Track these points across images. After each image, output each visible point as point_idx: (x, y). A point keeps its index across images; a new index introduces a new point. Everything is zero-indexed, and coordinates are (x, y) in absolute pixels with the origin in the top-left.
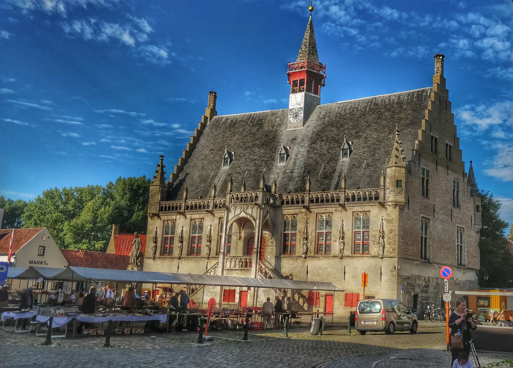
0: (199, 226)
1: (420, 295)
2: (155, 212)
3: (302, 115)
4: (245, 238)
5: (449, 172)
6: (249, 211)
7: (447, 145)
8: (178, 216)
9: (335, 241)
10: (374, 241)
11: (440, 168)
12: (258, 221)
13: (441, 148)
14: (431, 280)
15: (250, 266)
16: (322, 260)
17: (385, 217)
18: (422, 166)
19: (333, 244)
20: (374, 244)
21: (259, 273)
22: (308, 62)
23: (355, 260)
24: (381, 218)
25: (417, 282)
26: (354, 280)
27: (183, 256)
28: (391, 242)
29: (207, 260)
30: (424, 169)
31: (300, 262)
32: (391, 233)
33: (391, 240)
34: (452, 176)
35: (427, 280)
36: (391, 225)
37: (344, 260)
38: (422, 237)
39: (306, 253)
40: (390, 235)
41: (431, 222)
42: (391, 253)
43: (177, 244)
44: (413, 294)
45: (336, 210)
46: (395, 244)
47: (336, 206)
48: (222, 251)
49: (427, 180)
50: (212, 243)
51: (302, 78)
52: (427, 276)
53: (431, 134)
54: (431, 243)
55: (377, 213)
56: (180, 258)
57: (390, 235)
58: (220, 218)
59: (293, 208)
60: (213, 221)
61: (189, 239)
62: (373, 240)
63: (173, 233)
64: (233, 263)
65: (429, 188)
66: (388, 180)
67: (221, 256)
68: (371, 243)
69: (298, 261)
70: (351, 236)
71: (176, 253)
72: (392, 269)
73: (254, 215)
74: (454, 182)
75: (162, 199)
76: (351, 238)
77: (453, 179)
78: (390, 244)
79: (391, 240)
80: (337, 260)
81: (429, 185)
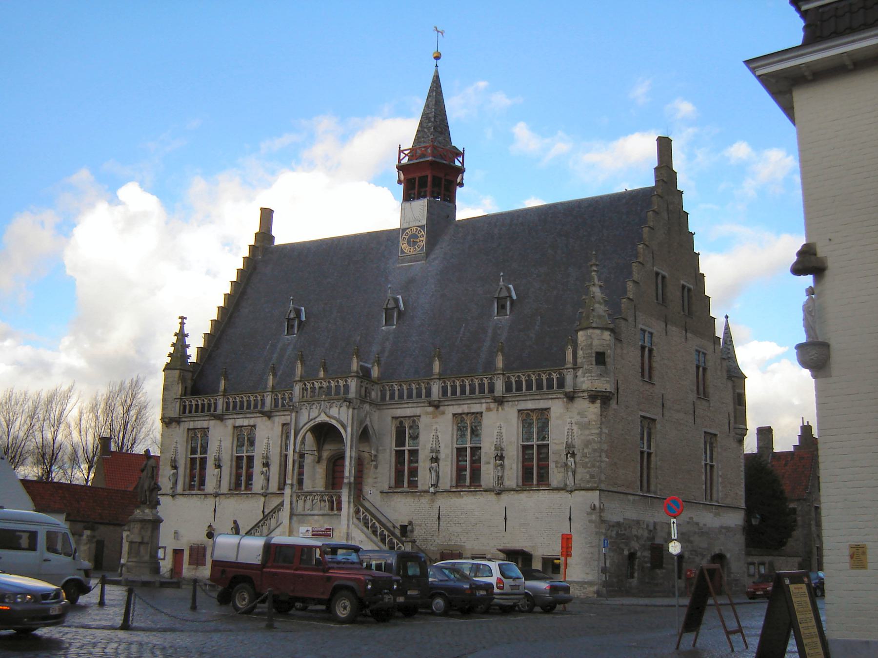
0: (248, 439)
1: (639, 554)
2: (173, 415)
3: (424, 239)
4: (329, 460)
5: (689, 335)
6: (334, 411)
7: (684, 287)
8: (212, 423)
9: (488, 463)
10: (557, 462)
11: (673, 329)
12: (349, 429)
13: (674, 294)
14: (658, 528)
15: (339, 509)
16: (465, 497)
17: (577, 418)
18: (641, 326)
19: (484, 468)
21: (355, 520)
22: (434, 148)
23: (523, 496)
25: (634, 532)
26: (524, 530)
28: (587, 463)
29: (263, 499)
30: (644, 331)
31: (425, 500)
33: (587, 460)
34: (695, 342)
35: (651, 528)
36: (587, 432)
37: (505, 497)
38: (642, 453)
39: (435, 485)
40: (586, 451)
41: (658, 426)
42: (588, 482)
43: (211, 471)
44: (626, 553)
47: (488, 401)
48: (289, 481)
49: (651, 351)
50: (271, 467)
51: (423, 174)
52: (651, 520)
53: (655, 269)
54: (659, 463)
56: (216, 495)
57: (586, 451)
58: (284, 425)
59: (410, 405)
60: (272, 429)
61: (232, 460)
62: (555, 459)
63: (204, 450)
64: (309, 502)
65: (654, 365)
66: (580, 353)
67: (288, 491)
68: (552, 465)
70: (515, 453)
71: (210, 485)
72: (589, 510)
73: (344, 419)
74: (698, 352)
75: (185, 394)
76: (515, 457)
77: (695, 348)
78: (585, 466)
79: (587, 460)
80: (492, 497)
81: (655, 359)
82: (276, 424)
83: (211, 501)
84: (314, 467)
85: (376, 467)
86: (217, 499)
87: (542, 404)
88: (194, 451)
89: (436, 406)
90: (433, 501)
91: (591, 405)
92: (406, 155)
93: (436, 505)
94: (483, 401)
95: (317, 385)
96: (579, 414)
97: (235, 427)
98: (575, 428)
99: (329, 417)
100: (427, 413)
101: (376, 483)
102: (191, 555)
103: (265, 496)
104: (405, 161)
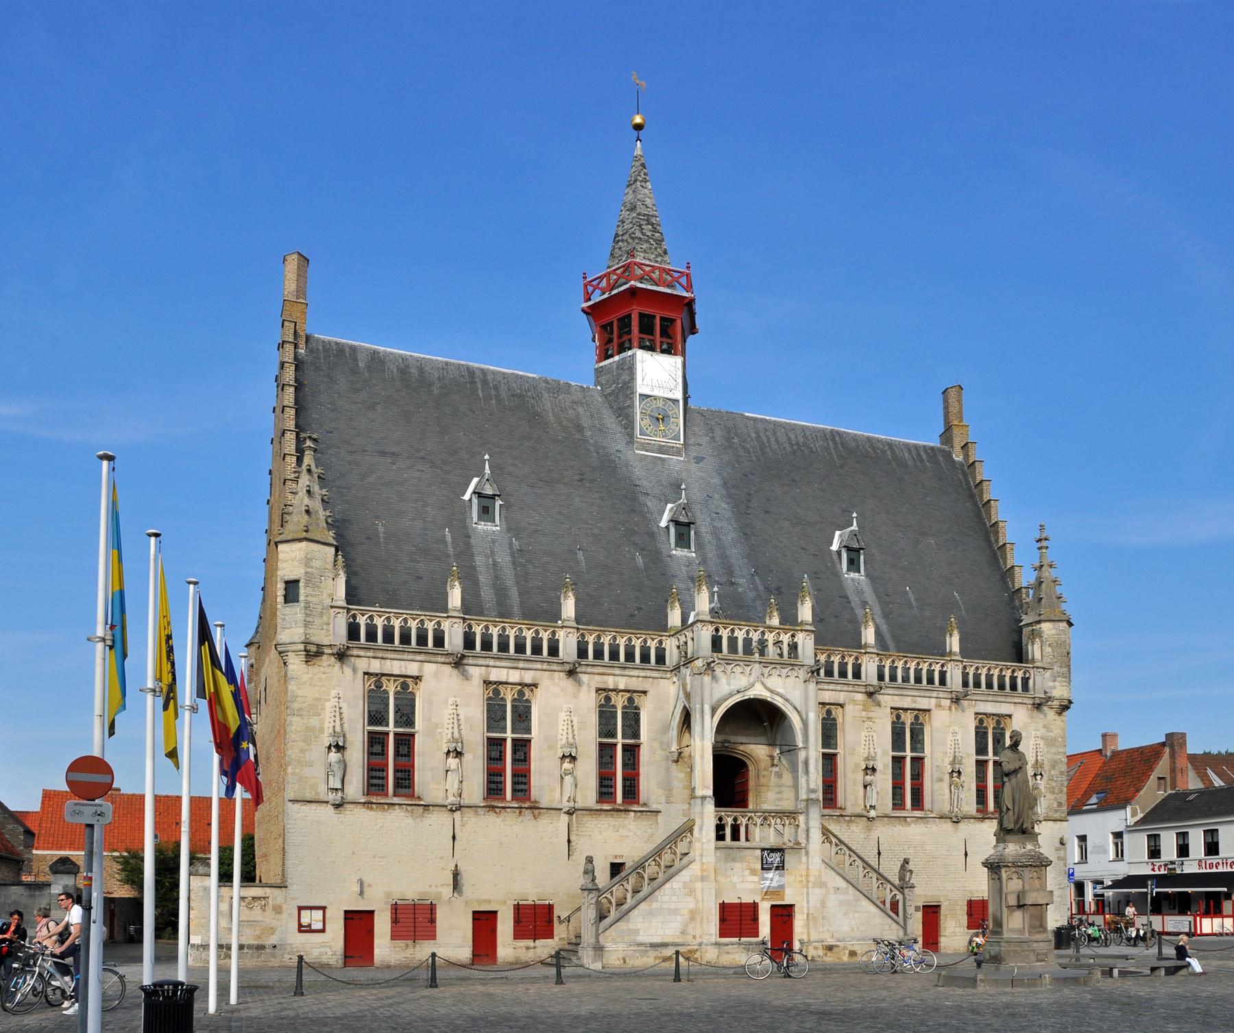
16: (913, 825)
17: (1042, 731)
27: (466, 801)
29: (565, 818)
32: (1053, 767)
36: (1053, 750)
37: (962, 826)
40: (1053, 772)
42: (1056, 811)
45: (939, 706)
46: (1061, 792)
55: (1026, 720)
69: (854, 827)
72: (1058, 845)
80: (947, 826)
83: (439, 822)
84: (668, 770)
86: (457, 815)
88: (376, 717)
90: (869, 829)
91: (1057, 717)
94: (935, 694)
95: (771, 637)
96: (1044, 727)
97: (487, 683)
98: (1040, 741)
99: (772, 691)
102: (395, 921)
103: (570, 813)
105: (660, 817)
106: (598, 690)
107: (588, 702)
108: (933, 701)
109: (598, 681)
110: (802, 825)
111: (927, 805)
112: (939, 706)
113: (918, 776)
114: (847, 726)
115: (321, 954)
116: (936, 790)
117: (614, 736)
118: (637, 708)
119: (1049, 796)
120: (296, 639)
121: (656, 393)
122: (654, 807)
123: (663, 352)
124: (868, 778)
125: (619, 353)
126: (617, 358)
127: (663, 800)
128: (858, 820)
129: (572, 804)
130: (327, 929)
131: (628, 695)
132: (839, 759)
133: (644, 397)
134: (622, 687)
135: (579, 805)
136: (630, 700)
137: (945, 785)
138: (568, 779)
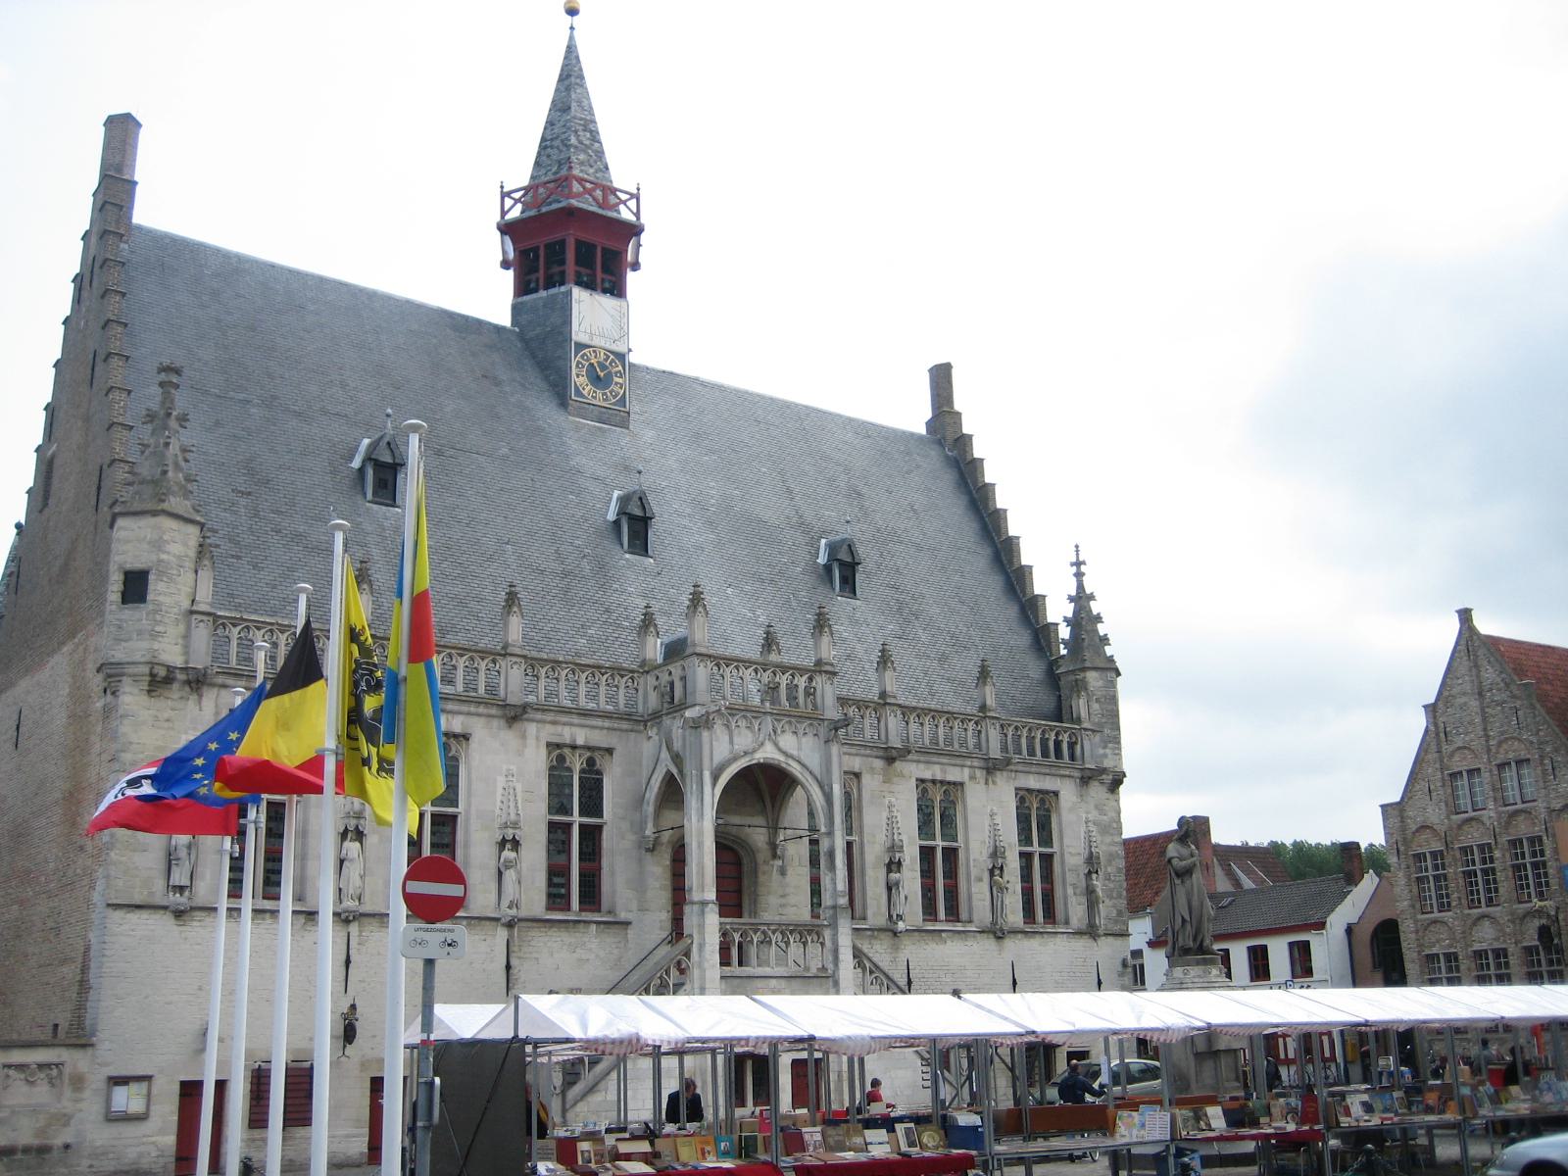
9: (980, 880)
10: (1074, 886)
17: (1094, 815)
20: (1075, 894)
23: (1035, 943)
24: (1084, 816)
28: (1111, 890)
29: (502, 934)
32: (1110, 862)
46: (1120, 896)
55: (1074, 799)
60: (520, 753)
72: (1120, 969)
79: (1112, 885)
80: (989, 943)
82: (531, 741)
84: (640, 860)
85: (783, 872)
86: (354, 928)
87: (1048, 784)
89: (891, 756)
90: (896, 948)
92: (516, 201)
93: (902, 957)
98: (1092, 828)
100: (872, 770)
101: (782, 906)
104: (516, 213)
105: (631, 932)
106: (549, 745)
107: (537, 761)
108: (966, 771)
109: (549, 733)
110: (828, 943)
111: (964, 916)
112: (972, 778)
113: (951, 873)
114: (865, 803)
115: (141, 1155)
116: (976, 893)
117: (568, 812)
118: (599, 773)
119: (1107, 901)
120: (138, 658)
121: (596, 342)
122: (623, 916)
123: (605, 291)
124: (894, 876)
125: (546, 288)
126: (543, 294)
127: (634, 906)
128: (883, 935)
129: (513, 912)
130: (152, 1113)
131: (589, 754)
132: (961, 854)
133: (580, 346)
134: (580, 741)
135: (524, 913)
136: (591, 762)
137: (985, 886)
138: (510, 876)
